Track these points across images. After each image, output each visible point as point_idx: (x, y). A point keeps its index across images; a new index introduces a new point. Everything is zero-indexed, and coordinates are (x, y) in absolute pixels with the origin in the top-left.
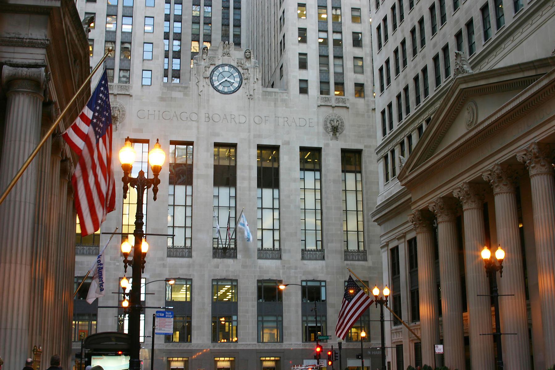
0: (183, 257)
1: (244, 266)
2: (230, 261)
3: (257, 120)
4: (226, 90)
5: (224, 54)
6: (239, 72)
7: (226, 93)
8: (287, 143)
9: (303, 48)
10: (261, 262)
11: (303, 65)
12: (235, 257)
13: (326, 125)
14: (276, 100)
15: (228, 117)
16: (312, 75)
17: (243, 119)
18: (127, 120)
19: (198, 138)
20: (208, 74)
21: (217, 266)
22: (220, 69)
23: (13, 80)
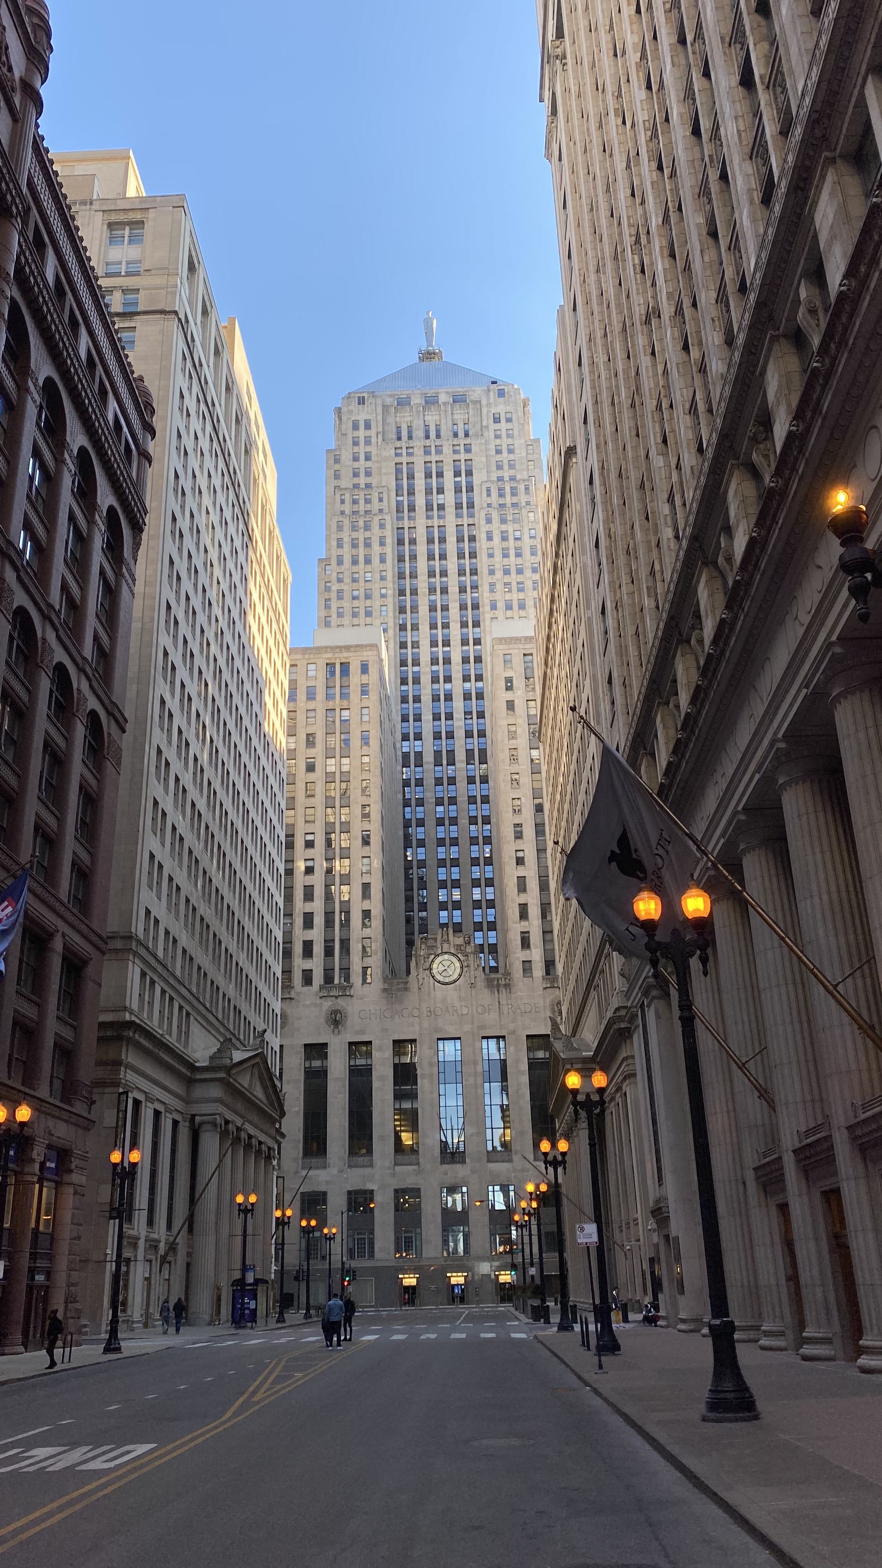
0: (410, 1164)
1: (473, 1171)
2: (458, 1167)
3: (480, 1010)
4: (447, 980)
5: (443, 941)
6: (459, 960)
7: (447, 984)
8: (513, 1032)
9: (524, 926)
10: (491, 1165)
11: (525, 943)
12: (464, 1162)
13: (553, 1008)
14: (498, 985)
15: (450, 1009)
16: (536, 954)
17: (465, 1011)
18: (349, 1022)
19: (420, 1035)
20: (427, 964)
21: (446, 1174)
22: (440, 959)
23: (202, 1124)
